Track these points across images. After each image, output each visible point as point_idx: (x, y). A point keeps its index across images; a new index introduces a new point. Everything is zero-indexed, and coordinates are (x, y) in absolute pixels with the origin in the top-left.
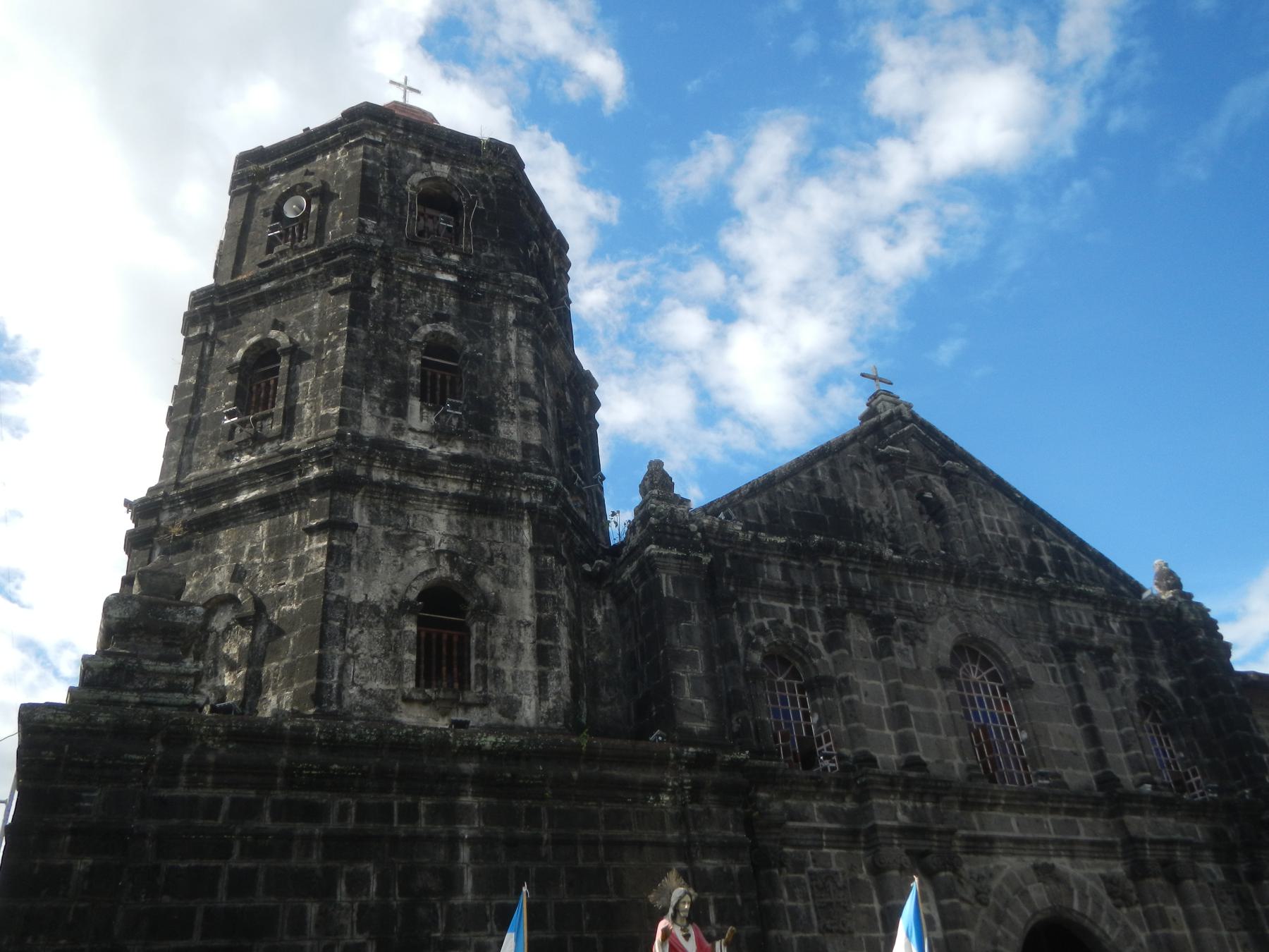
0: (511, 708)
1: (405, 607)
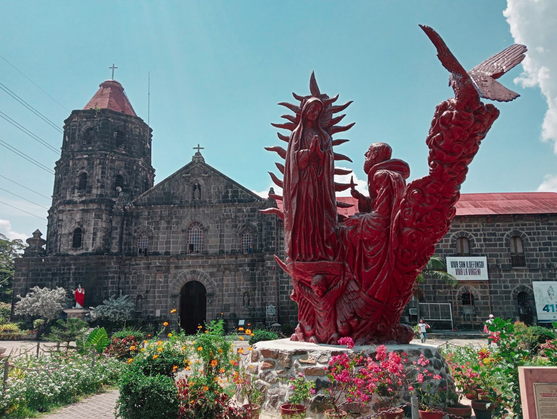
0: (87, 249)
1: (70, 234)
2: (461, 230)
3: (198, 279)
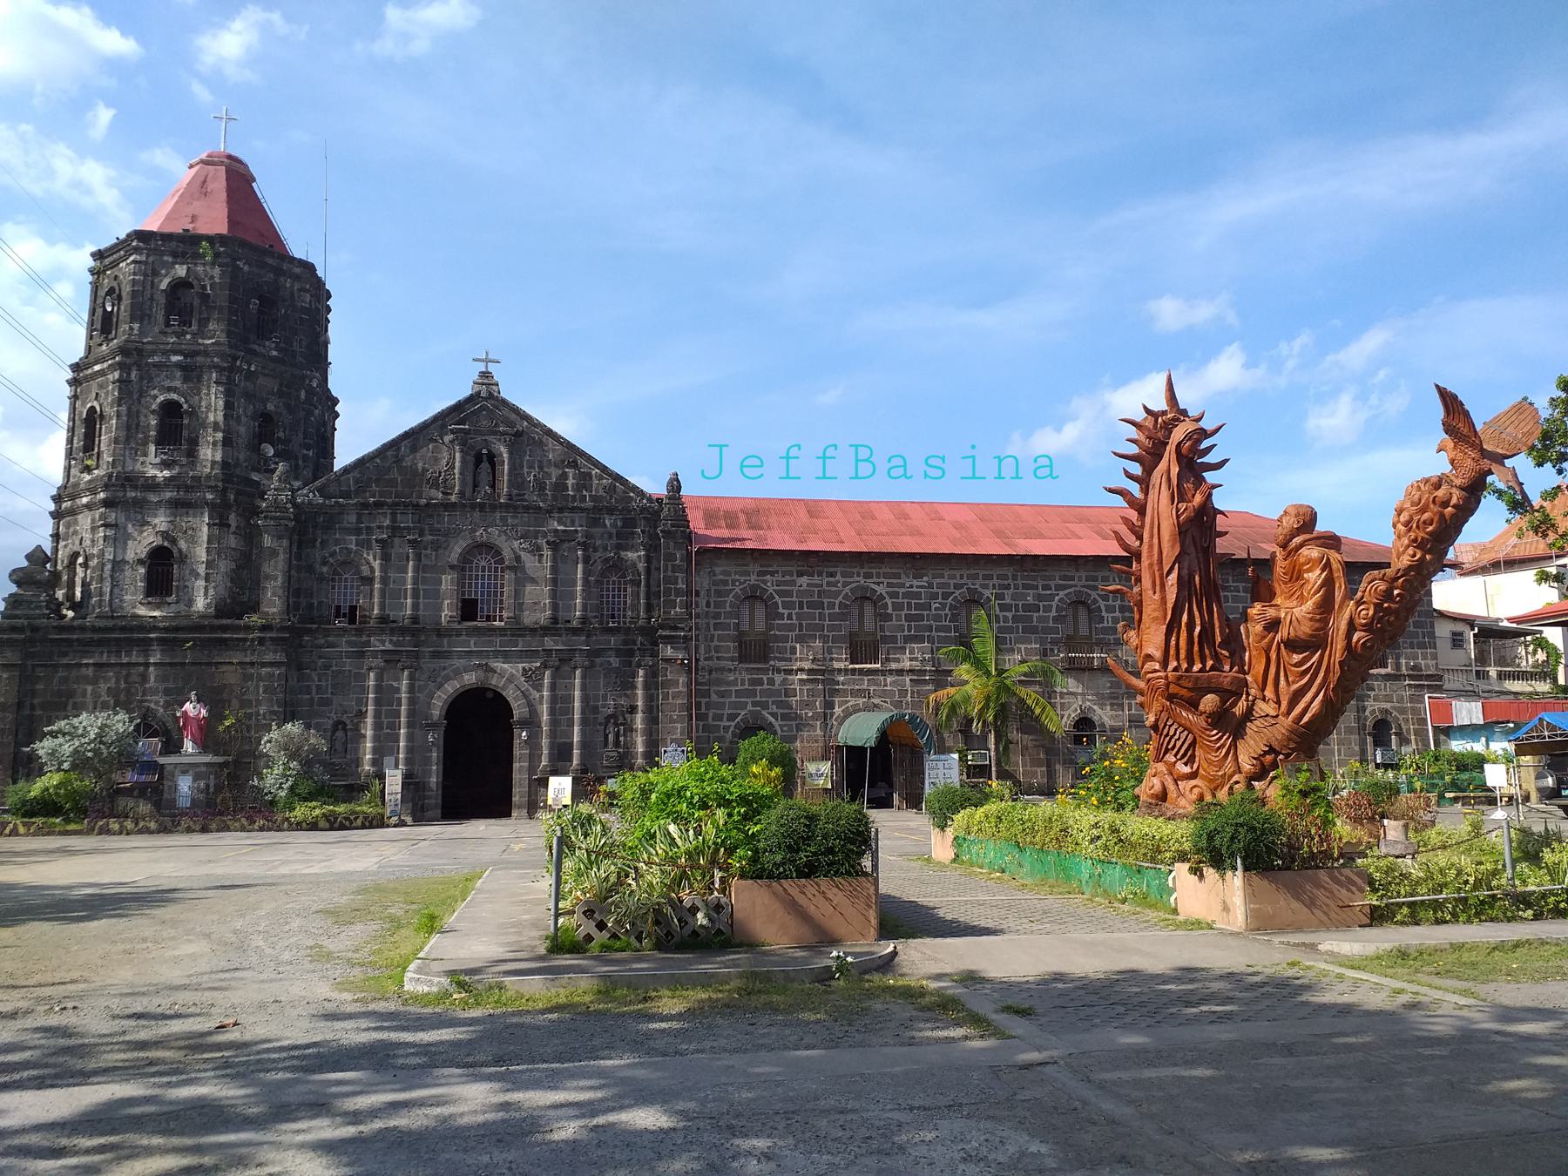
0: (190, 602)
1: (140, 562)
2: (1076, 586)
3: (494, 681)
